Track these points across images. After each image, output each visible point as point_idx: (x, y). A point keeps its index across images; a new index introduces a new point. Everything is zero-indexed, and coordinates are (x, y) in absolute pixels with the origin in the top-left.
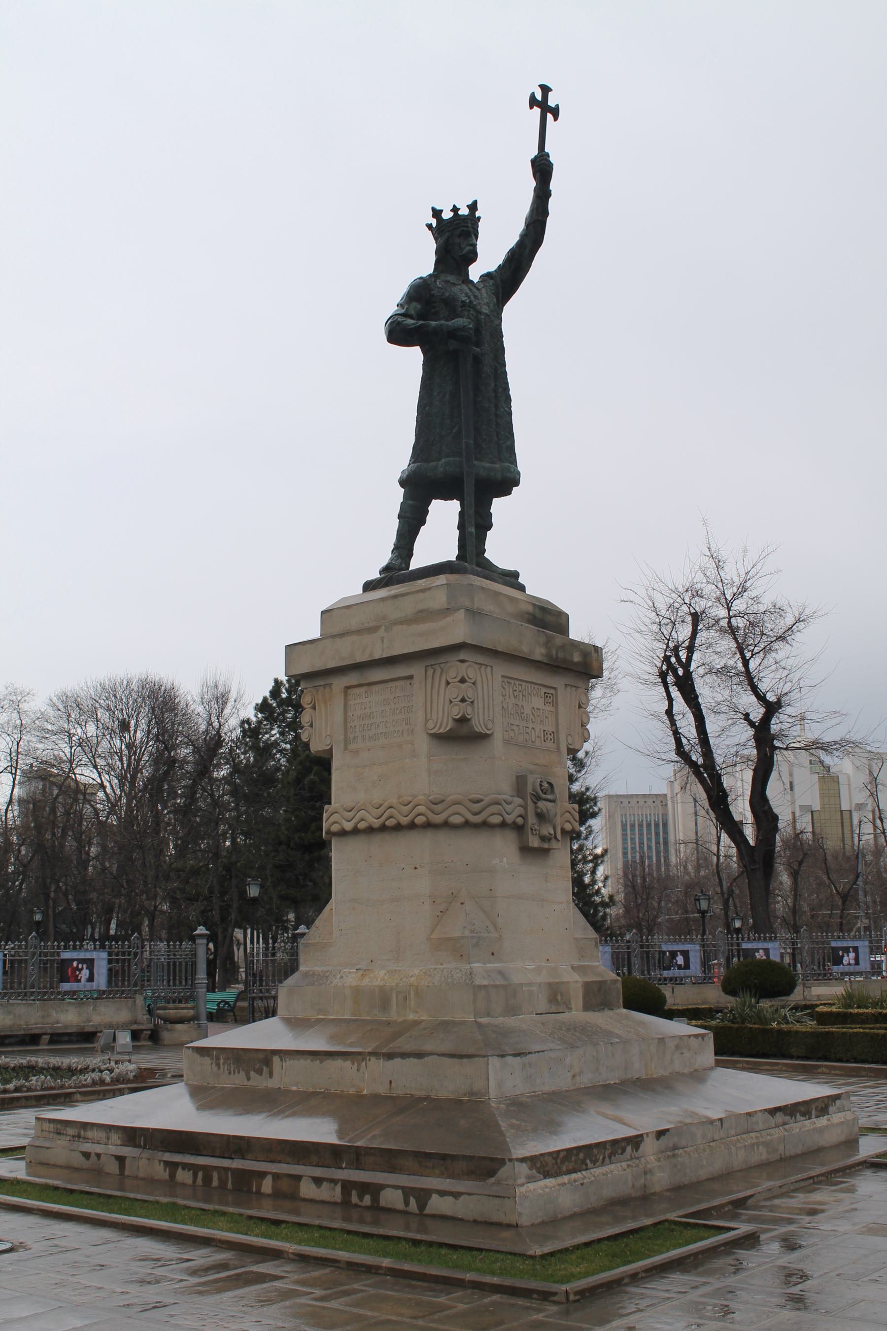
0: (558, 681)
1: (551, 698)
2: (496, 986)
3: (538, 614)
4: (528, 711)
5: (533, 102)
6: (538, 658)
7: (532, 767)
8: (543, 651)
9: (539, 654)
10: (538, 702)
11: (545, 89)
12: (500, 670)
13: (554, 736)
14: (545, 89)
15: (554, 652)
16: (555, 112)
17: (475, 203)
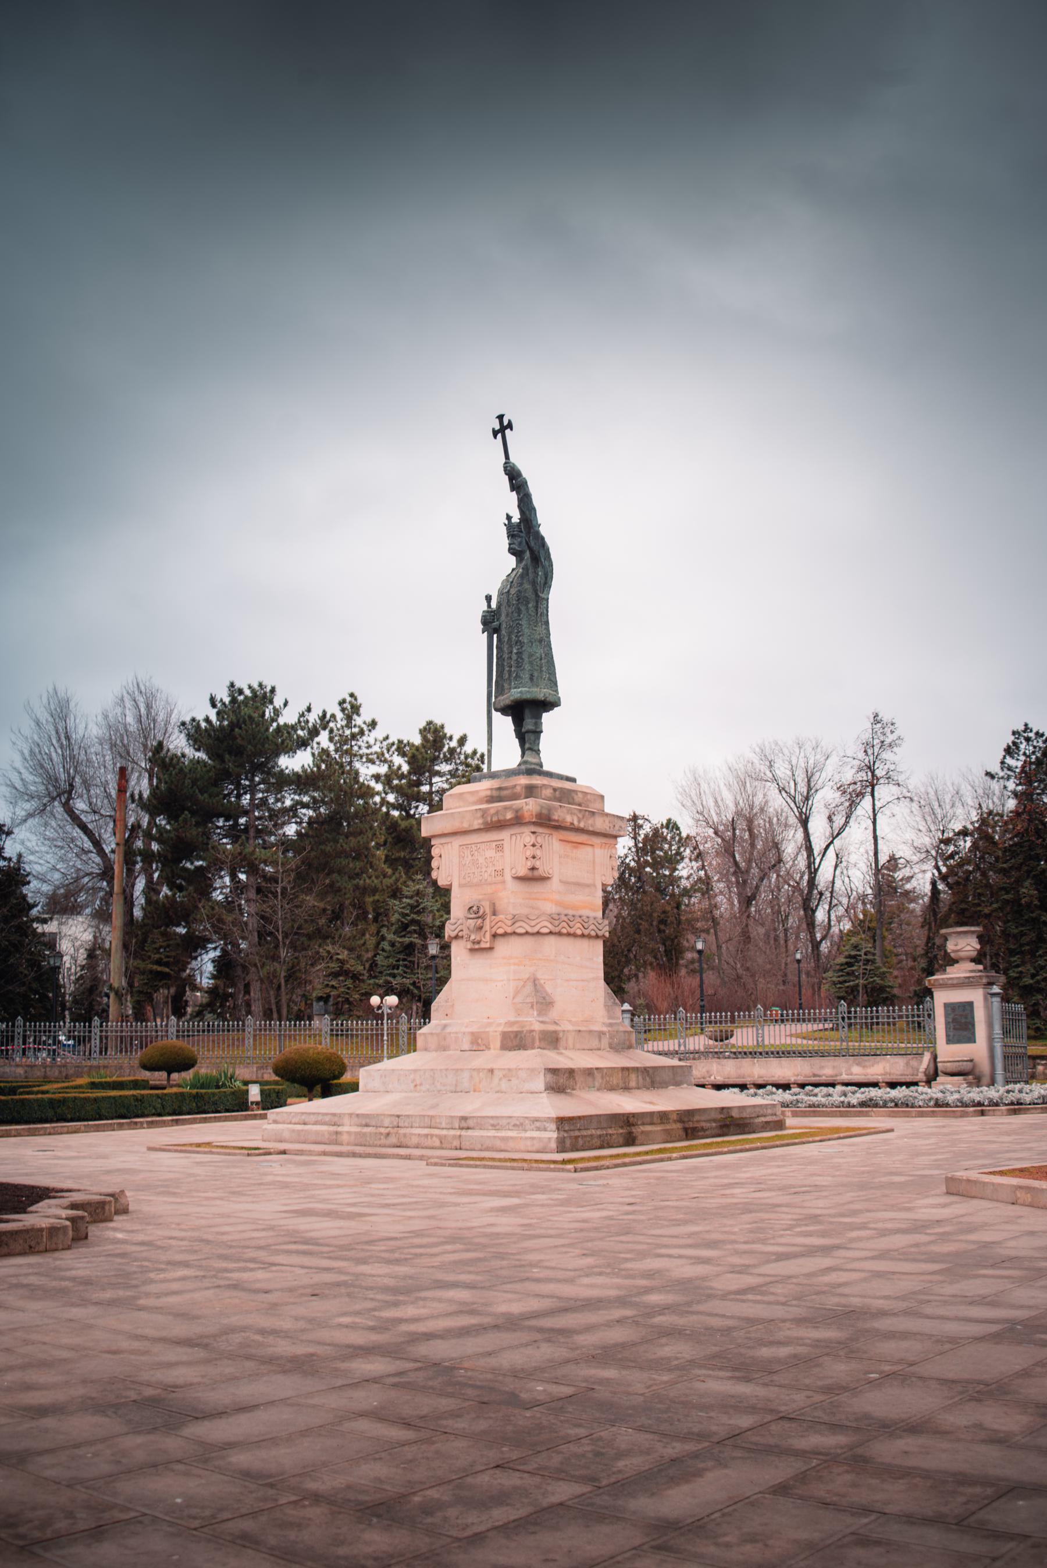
0: (505, 835)
1: (500, 848)
2: (432, 1034)
3: (495, 793)
4: (481, 860)
5: (495, 434)
6: (476, 827)
7: (480, 897)
8: (480, 821)
9: (477, 823)
10: (491, 853)
11: (501, 417)
12: (457, 842)
13: (501, 873)
14: (501, 417)
15: (489, 819)
16: (510, 426)
17: (507, 515)
